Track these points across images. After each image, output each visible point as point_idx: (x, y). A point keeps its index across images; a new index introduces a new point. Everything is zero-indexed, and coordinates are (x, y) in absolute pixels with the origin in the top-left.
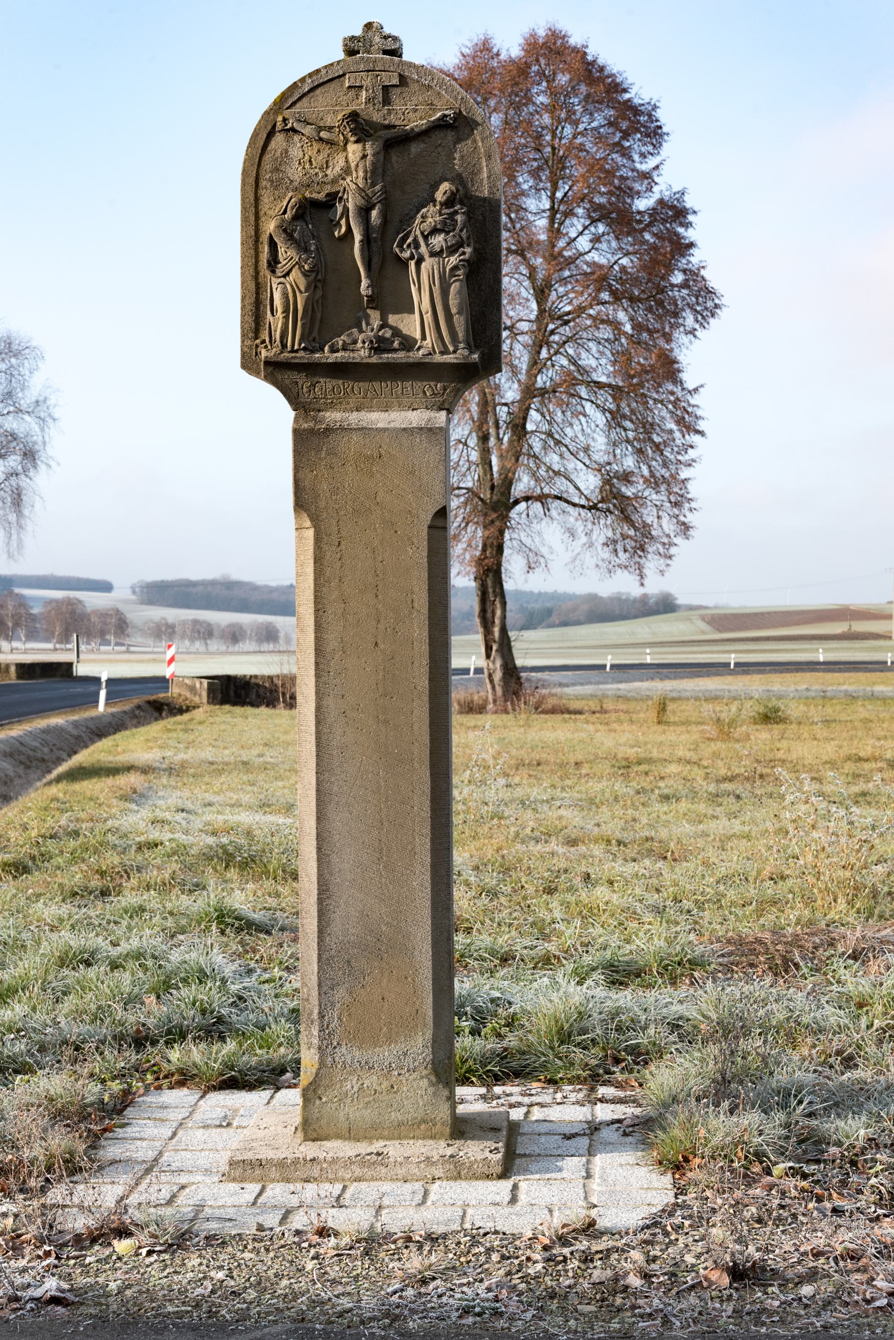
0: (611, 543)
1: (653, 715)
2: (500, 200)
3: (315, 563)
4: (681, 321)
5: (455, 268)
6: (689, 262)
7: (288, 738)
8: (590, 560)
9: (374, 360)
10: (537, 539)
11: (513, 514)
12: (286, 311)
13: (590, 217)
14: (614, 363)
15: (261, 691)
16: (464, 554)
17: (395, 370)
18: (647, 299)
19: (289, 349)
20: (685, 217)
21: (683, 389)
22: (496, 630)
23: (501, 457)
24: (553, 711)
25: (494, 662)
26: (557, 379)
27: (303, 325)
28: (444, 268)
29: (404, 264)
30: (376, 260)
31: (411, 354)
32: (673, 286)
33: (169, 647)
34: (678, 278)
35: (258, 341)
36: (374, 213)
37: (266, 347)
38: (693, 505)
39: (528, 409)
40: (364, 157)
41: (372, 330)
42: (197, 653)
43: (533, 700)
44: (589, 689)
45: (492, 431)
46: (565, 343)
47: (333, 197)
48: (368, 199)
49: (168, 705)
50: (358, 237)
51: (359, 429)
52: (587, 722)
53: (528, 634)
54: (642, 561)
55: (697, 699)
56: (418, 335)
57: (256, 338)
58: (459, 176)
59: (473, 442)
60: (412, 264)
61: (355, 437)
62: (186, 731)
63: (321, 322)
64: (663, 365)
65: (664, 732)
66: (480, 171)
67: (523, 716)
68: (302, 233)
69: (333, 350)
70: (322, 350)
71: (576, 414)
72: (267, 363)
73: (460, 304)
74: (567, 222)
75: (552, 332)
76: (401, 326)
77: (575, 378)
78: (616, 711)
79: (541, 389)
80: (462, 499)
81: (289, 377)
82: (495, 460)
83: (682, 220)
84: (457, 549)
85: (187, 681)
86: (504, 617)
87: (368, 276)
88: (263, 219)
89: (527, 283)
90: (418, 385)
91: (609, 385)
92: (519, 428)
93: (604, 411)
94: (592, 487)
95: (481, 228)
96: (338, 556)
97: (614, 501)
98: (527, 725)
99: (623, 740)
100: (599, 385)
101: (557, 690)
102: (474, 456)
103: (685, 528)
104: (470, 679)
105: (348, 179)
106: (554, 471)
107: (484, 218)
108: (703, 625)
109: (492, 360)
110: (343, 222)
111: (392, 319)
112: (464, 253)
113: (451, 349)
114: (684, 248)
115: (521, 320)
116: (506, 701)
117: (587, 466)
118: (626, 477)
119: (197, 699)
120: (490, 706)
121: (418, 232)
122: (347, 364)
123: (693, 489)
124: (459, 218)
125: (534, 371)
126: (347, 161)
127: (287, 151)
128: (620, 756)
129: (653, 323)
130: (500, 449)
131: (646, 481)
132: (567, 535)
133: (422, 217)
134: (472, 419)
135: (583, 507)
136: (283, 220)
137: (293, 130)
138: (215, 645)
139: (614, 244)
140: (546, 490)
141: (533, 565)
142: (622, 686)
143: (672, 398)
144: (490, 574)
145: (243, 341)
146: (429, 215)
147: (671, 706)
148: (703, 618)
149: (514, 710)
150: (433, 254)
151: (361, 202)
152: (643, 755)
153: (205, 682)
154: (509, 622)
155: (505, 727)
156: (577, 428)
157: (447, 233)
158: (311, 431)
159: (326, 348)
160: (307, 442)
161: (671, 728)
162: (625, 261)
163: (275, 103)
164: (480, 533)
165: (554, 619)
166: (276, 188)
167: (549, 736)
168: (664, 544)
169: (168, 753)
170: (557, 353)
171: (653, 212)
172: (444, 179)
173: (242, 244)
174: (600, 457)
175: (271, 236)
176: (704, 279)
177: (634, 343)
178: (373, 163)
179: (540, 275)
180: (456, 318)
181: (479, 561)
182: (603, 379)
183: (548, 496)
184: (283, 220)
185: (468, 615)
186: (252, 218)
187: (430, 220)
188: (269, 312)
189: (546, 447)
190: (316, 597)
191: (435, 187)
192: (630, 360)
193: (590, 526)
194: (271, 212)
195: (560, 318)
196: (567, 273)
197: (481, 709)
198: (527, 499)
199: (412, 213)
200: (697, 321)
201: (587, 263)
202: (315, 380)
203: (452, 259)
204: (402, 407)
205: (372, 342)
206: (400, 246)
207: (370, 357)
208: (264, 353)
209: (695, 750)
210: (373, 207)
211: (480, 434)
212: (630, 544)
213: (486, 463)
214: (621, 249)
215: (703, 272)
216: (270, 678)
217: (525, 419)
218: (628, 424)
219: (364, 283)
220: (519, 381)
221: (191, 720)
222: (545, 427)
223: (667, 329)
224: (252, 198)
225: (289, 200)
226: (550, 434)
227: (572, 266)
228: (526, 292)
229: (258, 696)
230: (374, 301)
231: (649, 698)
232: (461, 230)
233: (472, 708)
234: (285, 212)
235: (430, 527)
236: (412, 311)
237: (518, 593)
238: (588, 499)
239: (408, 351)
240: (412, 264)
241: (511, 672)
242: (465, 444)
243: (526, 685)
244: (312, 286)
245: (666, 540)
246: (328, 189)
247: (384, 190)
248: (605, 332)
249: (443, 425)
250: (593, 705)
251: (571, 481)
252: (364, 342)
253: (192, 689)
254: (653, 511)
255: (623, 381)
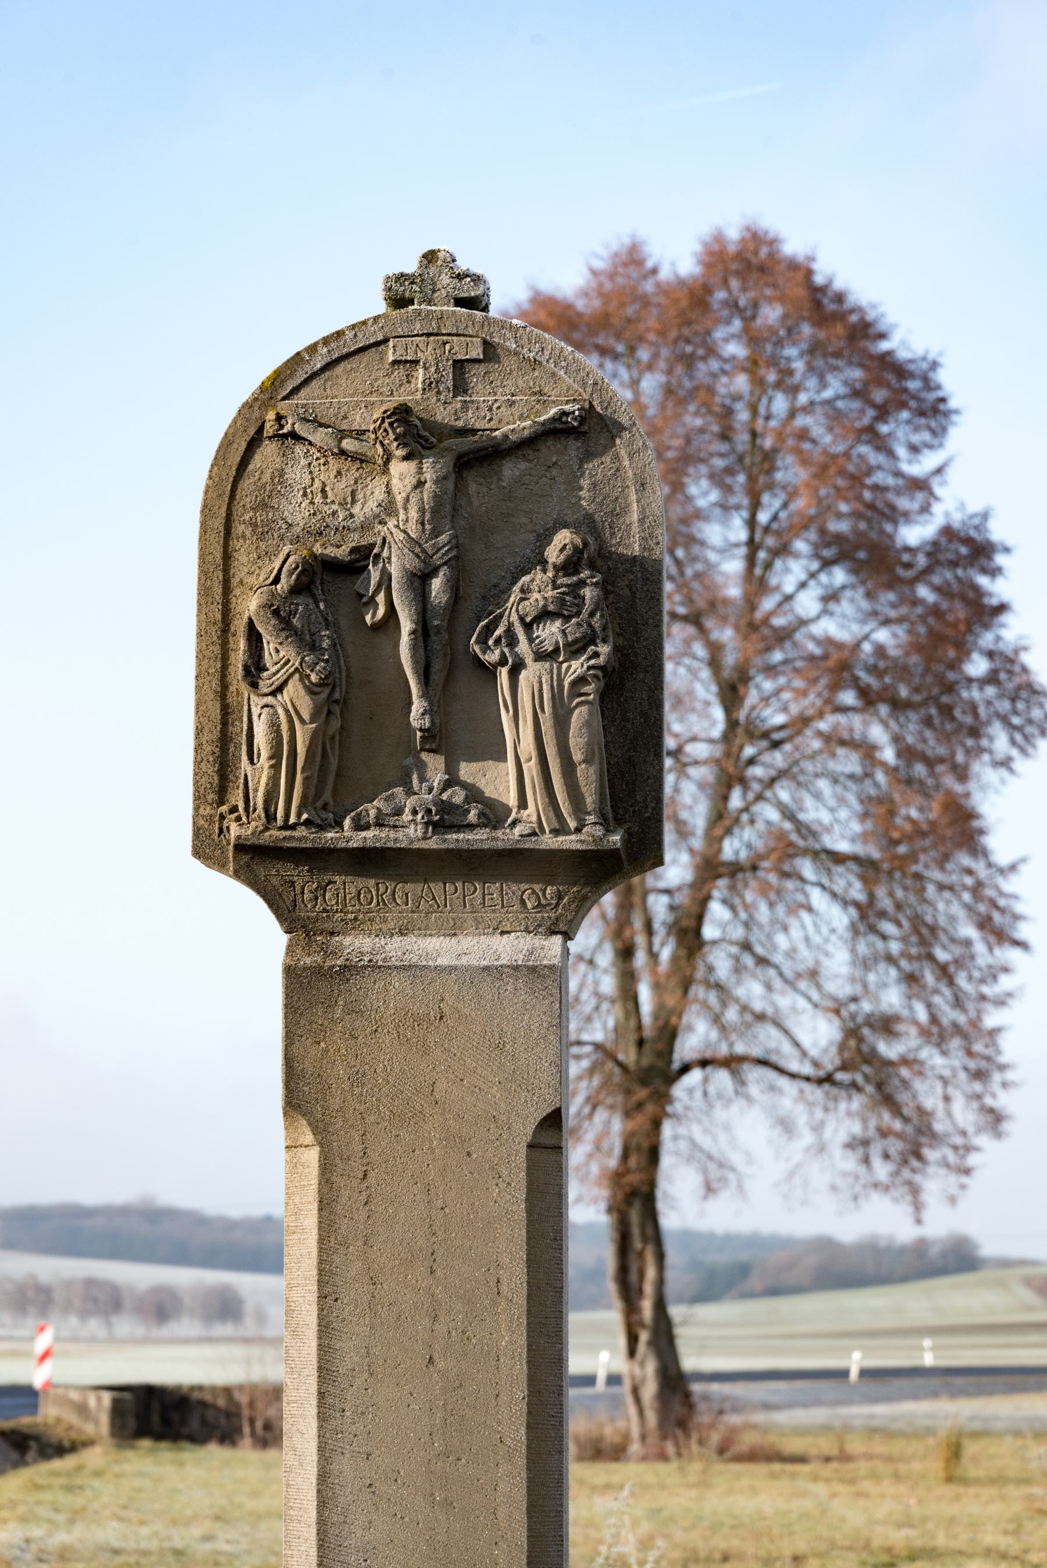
0: (859, 1144)
1: (935, 1466)
2: (660, 562)
3: (320, 1210)
4: (984, 742)
5: (581, 681)
6: (998, 638)
7: (259, 1505)
8: (819, 1175)
9: (433, 843)
10: (723, 1138)
11: (679, 1090)
12: (276, 755)
13: (817, 556)
14: (864, 816)
15: (210, 1414)
16: (587, 1164)
17: (467, 862)
18: (924, 704)
19: (280, 822)
20: (990, 558)
21: (990, 865)
22: (647, 1307)
23: (657, 987)
24: (752, 1456)
25: (642, 1364)
26: (759, 845)
27: (306, 780)
28: (560, 681)
29: (489, 672)
30: (438, 666)
31: (499, 833)
32: (970, 680)
33: (42, 1329)
34: (977, 666)
35: (224, 809)
36: (437, 584)
37: (238, 819)
38: (1010, 1076)
39: (708, 898)
40: (420, 484)
41: (430, 790)
42: (92, 1340)
43: (715, 1438)
44: (818, 1415)
45: (640, 940)
46: (773, 781)
47: (364, 555)
48: (425, 558)
49: (36, 1438)
50: (406, 625)
51: (404, 968)
52: (815, 1478)
53: (706, 1311)
54: (918, 1178)
55: (1018, 1434)
56: (512, 800)
57: (221, 803)
58: (589, 519)
59: (606, 958)
60: (504, 673)
61: (397, 982)
62: (69, 1489)
63: (338, 774)
64: (952, 823)
65: (958, 1498)
66: (626, 509)
67: (696, 1467)
68: (307, 616)
69: (359, 826)
70: (339, 824)
71: (794, 909)
72: (240, 848)
73: (589, 745)
74: (778, 564)
75: (752, 761)
76: (481, 784)
77: (791, 844)
78: (869, 1457)
79: (730, 864)
80: (585, 1063)
81: (277, 872)
82: (645, 993)
83: (984, 562)
84: (577, 1154)
85: (74, 1395)
86: (660, 1282)
87: (425, 695)
88: (237, 592)
89: (705, 673)
90: (513, 889)
91: (855, 858)
92: (689, 934)
93: (845, 903)
94: (823, 1043)
95: (625, 613)
96: (363, 1197)
97: (863, 1067)
98: (704, 1484)
99: (882, 1511)
100: (839, 858)
101: (759, 1417)
102: (608, 984)
103: (994, 1120)
104: (597, 1397)
105: (391, 523)
106: (753, 1013)
107: (634, 595)
108: (1028, 1296)
109: (645, 850)
110: (381, 598)
111: (466, 771)
112: (596, 655)
113: (572, 824)
114: (987, 612)
115: (694, 739)
116: (664, 1437)
117: (816, 1006)
118: (887, 1025)
119: (89, 1429)
120: (635, 1448)
121: (514, 618)
122: (383, 851)
123: (1009, 1048)
124: (588, 593)
125: (718, 831)
126: (389, 492)
127: (282, 473)
128: (876, 1543)
129: (934, 747)
130: (654, 972)
131: (925, 1033)
132: (778, 1130)
133: (522, 591)
134: (604, 916)
135: (808, 1079)
136: (273, 595)
137: (294, 436)
138: (125, 1326)
139: (865, 605)
140: (740, 1048)
141: (714, 1185)
142: (881, 1410)
143: (969, 881)
144: (636, 1201)
145: (196, 809)
146: (534, 586)
147: (971, 1448)
148: (1028, 1282)
149: (679, 1455)
150: (540, 656)
151: (412, 563)
152: (918, 1543)
153: (107, 1398)
154: (671, 1289)
155: (663, 1487)
156: (796, 933)
157: (567, 619)
158: (318, 971)
159: (347, 823)
160: (311, 990)
161: (972, 1490)
162: (882, 636)
163: (262, 389)
164: (617, 1125)
165: (754, 1282)
166: (262, 537)
167: (745, 1505)
168: (955, 1148)
169: (37, 1532)
170: (760, 797)
171: (934, 549)
172: (561, 524)
173: (199, 635)
174: (839, 986)
175: (251, 622)
176: (1025, 670)
177: (899, 781)
178: (436, 496)
179: (730, 659)
180: (581, 770)
181: (617, 1178)
182: (843, 846)
183: (742, 1059)
184: (273, 595)
185: (594, 1275)
186: (218, 590)
187: (536, 595)
188: (244, 758)
189: (738, 969)
190: (321, 1272)
191: (545, 538)
192: (892, 813)
193: (819, 1113)
194: (251, 580)
195: (765, 735)
196: (777, 656)
197: (617, 1452)
198: (704, 1063)
199: (504, 584)
200: (1013, 742)
201: (813, 638)
202: (326, 878)
203: (575, 664)
204: (482, 928)
205: (429, 811)
206: (483, 641)
207: (425, 838)
208: (234, 830)
209: (1016, 1533)
210: (434, 572)
211: (620, 945)
212: (895, 1146)
213: (628, 995)
214: (875, 613)
215: (1025, 658)
216: (227, 1391)
217: (700, 918)
218: (889, 928)
219: (418, 706)
220: (691, 851)
221: (79, 1468)
222: (738, 933)
223: (960, 757)
224: (219, 555)
225: (284, 560)
226: (746, 946)
227: (788, 645)
228: (706, 691)
229: (204, 1423)
230: (435, 739)
231: (930, 1431)
232: (592, 614)
233: (605, 1451)
234: (277, 580)
235: (530, 1146)
236: (502, 757)
237: (687, 1236)
238: (816, 1064)
239: (495, 828)
240: (504, 673)
241: (674, 1383)
242: (591, 962)
243: (701, 1407)
244: (323, 712)
245: (958, 1140)
246: (354, 540)
247: (456, 544)
248: (849, 762)
249: (556, 961)
250: (826, 1445)
251: (786, 1032)
252: (415, 812)
253: (82, 1409)
254: (937, 1086)
255: (881, 849)
